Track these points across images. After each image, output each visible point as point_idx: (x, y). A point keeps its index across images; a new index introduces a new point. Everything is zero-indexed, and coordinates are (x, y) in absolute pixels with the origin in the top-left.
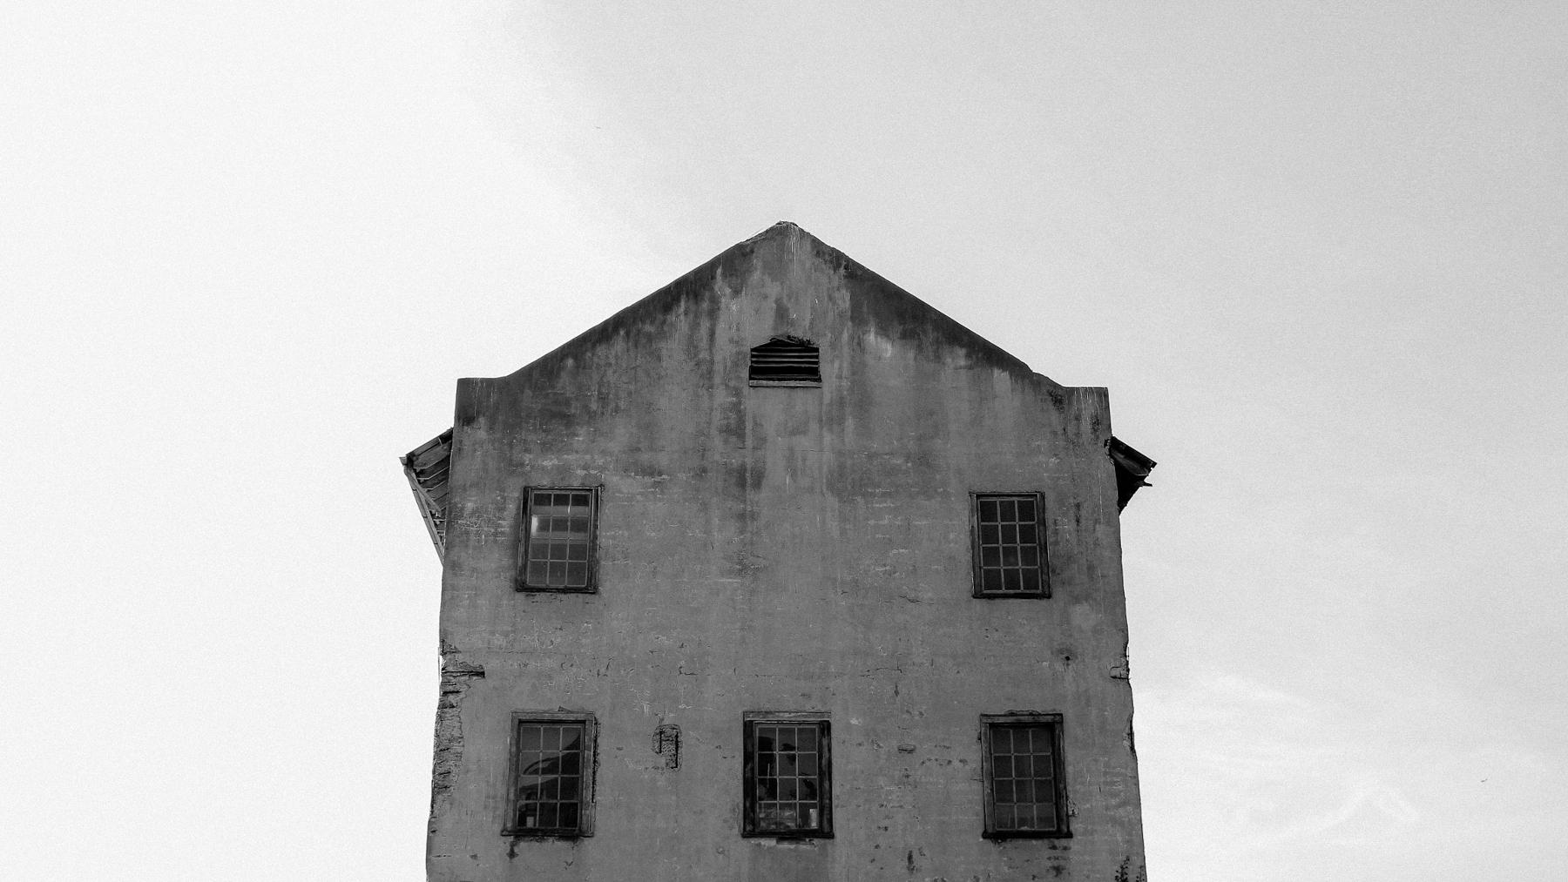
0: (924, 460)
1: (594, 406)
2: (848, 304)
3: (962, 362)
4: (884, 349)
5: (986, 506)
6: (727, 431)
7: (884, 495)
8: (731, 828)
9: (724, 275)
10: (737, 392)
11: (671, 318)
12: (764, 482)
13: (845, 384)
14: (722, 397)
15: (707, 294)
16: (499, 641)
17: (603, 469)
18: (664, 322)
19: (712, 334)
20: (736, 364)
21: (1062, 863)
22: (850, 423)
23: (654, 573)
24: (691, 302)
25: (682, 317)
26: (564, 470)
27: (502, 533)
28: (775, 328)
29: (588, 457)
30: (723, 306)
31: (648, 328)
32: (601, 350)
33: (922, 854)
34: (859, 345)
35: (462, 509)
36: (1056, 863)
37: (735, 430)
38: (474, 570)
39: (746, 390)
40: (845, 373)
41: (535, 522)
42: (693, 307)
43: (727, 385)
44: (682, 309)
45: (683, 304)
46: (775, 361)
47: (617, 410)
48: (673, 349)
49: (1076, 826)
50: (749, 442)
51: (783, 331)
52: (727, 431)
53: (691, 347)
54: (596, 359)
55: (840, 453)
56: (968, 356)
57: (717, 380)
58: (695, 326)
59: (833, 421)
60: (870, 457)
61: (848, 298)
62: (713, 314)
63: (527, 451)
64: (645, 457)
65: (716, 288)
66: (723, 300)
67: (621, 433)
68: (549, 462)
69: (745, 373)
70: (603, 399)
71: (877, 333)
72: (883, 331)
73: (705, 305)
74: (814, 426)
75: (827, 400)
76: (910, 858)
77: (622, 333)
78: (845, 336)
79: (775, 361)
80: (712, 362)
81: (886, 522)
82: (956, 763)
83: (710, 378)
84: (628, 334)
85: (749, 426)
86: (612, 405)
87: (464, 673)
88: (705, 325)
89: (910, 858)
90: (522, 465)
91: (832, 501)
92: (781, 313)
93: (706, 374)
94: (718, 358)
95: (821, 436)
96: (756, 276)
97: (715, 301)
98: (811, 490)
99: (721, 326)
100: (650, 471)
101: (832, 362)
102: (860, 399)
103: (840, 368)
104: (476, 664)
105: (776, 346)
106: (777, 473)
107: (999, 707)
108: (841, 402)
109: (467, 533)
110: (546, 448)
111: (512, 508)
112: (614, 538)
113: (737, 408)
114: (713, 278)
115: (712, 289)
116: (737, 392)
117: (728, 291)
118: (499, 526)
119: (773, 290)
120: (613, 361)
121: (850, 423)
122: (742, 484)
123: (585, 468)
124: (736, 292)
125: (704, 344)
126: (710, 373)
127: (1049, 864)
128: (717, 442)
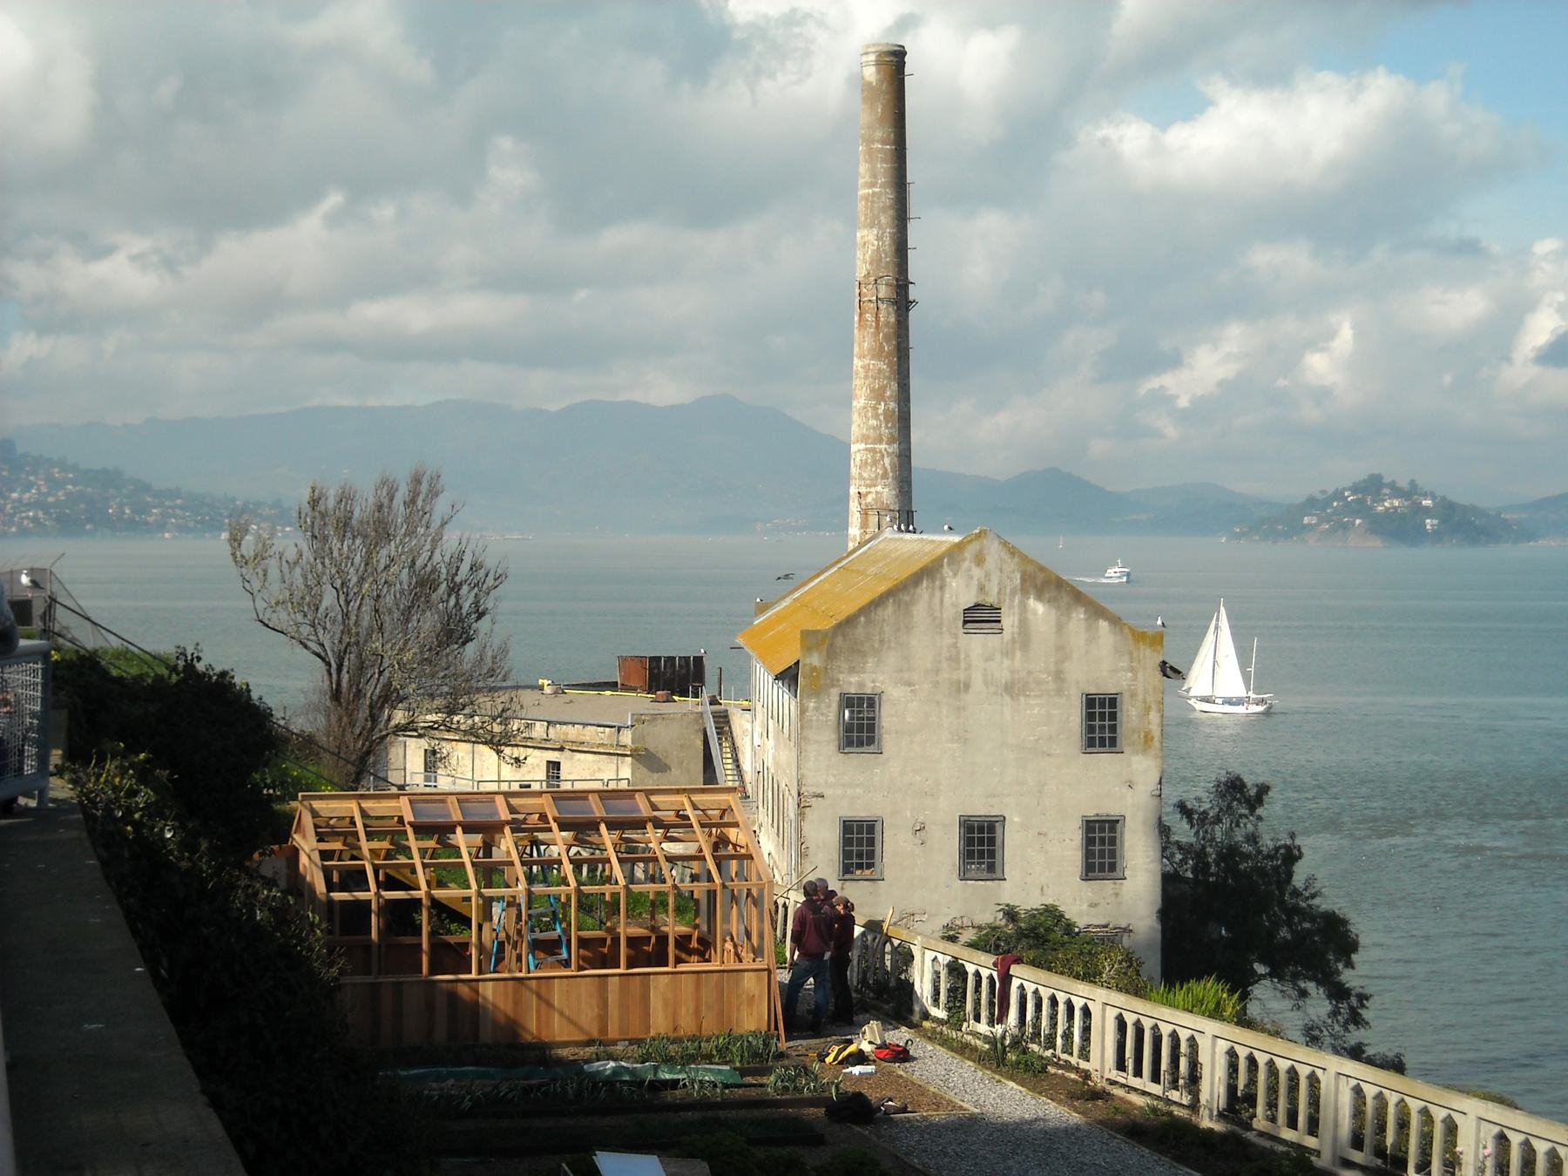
0: (1059, 676)
1: (876, 645)
2: (1019, 581)
3: (1082, 616)
4: (1038, 608)
5: (1090, 701)
6: (950, 659)
7: (1036, 696)
8: (952, 874)
9: (949, 564)
10: (956, 636)
11: (918, 591)
12: (970, 690)
13: (1016, 630)
14: (948, 640)
15: (939, 576)
16: (831, 779)
17: (882, 683)
18: (915, 593)
19: (942, 601)
20: (955, 619)
21: (1118, 891)
22: (1018, 654)
23: (912, 742)
24: (930, 581)
25: (925, 590)
26: (861, 684)
27: (830, 720)
28: (977, 597)
29: (874, 675)
30: (948, 583)
31: (906, 598)
32: (880, 611)
33: (1048, 887)
34: (1024, 607)
35: (808, 707)
36: (1115, 891)
37: (954, 659)
38: (816, 742)
39: (961, 635)
40: (1016, 624)
41: (847, 713)
42: (931, 585)
43: (950, 633)
44: (925, 585)
45: (925, 581)
46: (977, 615)
47: (889, 648)
48: (919, 611)
49: (1127, 873)
50: (963, 665)
51: (980, 600)
52: (950, 659)
53: (930, 607)
54: (877, 617)
55: (1012, 672)
56: (1086, 612)
57: (945, 629)
58: (932, 597)
59: (1007, 653)
60: (1029, 673)
61: (1019, 577)
62: (942, 588)
63: (841, 672)
64: (906, 675)
65: (944, 571)
66: (948, 579)
67: (892, 658)
68: (854, 679)
69: (960, 623)
70: (881, 641)
71: (1035, 599)
72: (1039, 598)
73: (938, 583)
74: (998, 657)
75: (1005, 640)
76: (1042, 888)
77: (891, 601)
78: (1017, 601)
79: (977, 615)
80: (942, 618)
81: (1036, 712)
82: (1068, 841)
83: (941, 629)
84: (894, 601)
85: (962, 657)
86: (886, 645)
87: (814, 796)
88: (938, 594)
89: (1042, 888)
90: (838, 680)
91: (1007, 698)
92: (981, 588)
93: (937, 626)
94: (945, 616)
95: (1002, 662)
96: (966, 565)
97: (943, 579)
98: (995, 693)
99: (947, 596)
100: (910, 684)
101: (1009, 616)
102: (1024, 637)
103: (1014, 621)
104: (819, 792)
105: (977, 607)
106: (977, 684)
107: (1091, 813)
108: (1013, 640)
109: (811, 720)
110: (852, 671)
111: (835, 706)
112: (890, 721)
113: (955, 645)
114: (942, 566)
115: (941, 573)
116: (956, 636)
117: (951, 574)
118: (828, 716)
119: (977, 572)
120: (886, 618)
121: (1018, 654)
122: (958, 691)
123: (873, 682)
124: (955, 575)
125: (937, 607)
126: (941, 625)
127: (1112, 892)
128: (945, 665)
